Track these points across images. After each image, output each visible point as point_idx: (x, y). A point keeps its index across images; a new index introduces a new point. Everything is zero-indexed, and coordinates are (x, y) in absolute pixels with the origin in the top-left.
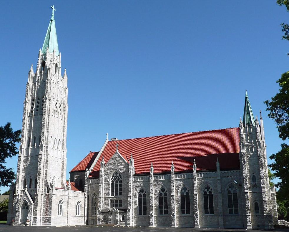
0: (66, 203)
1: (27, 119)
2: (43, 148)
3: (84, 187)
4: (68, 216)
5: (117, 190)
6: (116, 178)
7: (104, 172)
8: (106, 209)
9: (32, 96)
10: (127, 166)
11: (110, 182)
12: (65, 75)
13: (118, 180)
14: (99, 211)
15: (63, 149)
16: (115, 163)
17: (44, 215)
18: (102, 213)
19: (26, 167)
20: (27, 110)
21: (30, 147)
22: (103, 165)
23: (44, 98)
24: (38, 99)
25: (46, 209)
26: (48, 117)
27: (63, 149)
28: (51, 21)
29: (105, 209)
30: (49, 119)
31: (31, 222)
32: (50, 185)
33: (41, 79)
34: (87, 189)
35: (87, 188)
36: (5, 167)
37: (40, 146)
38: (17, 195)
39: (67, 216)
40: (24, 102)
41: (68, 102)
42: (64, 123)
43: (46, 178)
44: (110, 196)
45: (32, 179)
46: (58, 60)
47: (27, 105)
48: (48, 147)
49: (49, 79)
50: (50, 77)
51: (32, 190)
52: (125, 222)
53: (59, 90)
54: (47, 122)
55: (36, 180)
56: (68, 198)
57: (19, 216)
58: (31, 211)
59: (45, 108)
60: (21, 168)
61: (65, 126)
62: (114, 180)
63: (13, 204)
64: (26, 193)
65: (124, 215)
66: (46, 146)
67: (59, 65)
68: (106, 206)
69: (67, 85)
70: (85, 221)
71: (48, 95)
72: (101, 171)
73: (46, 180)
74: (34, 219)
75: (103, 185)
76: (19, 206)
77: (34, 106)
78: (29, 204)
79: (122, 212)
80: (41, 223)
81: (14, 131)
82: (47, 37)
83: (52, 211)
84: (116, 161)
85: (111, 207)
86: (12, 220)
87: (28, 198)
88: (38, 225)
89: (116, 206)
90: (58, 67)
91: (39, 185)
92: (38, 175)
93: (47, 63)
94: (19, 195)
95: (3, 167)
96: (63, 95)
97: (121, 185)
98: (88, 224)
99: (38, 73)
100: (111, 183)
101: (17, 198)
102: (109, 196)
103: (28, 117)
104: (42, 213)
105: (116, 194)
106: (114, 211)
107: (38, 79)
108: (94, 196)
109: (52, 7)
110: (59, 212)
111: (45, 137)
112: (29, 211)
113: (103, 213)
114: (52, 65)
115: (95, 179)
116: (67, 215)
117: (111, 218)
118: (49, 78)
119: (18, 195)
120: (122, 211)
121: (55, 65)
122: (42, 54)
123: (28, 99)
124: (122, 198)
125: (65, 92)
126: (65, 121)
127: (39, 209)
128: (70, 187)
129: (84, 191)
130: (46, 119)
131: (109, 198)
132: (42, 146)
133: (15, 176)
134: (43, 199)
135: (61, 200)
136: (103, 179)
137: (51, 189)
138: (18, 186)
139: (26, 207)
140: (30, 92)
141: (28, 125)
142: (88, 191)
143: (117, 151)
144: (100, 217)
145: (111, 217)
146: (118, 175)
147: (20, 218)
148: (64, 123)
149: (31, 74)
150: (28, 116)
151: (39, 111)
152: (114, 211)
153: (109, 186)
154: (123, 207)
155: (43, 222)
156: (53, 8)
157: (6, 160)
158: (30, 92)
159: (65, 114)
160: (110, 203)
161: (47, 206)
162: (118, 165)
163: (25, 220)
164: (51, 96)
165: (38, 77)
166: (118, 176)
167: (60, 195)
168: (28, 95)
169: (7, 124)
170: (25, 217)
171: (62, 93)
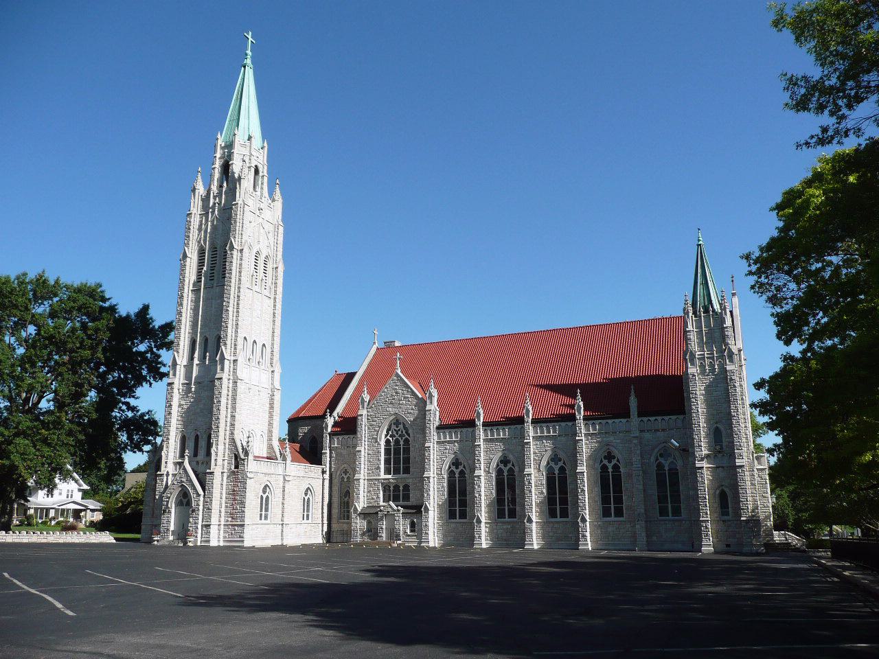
0: (278, 492)
1: (188, 297)
2: (226, 362)
5: (397, 462)
6: (395, 433)
7: (368, 419)
9: (199, 242)
10: (422, 405)
11: (383, 443)
13: (400, 438)
14: (356, 509)
16: (394, 399)
17: (227, 521)
18: (363, 516)
19: (185, 407)
20: (187, 275)
21: (196, 361)
22: (366, 404)
23: (227, 248)
24: (214, 249)
28: (245, 67)
29: (371, 505)
30: (238, 297)
31: (197, 537)
32: (241, 451)
33: (221, 202)
34: (328, 459)
35: (328, 456)
36: (136, 408)
37: (217, 359)
39: (281, 523)
41: (283, 256)
42: (275, 306)
44: (383, 476)
46: (261, 157)
47: (188, 264)
49: (239, 202)
50: (241, 199)
54: (236, 303)
55: (209, 437)
56: (285, 480)
57: (169, 522)
58: (199, 510)
59: (231, 270)
61: (276, 311)
63: (155, 495)
64: (185, 469)
65: (415, 520)
66: (233, 358)
67: (263, 171)
68: (373, 499)
69: (280, 218)
70: (324, 533)
71: (237, 239)
72: (359, 418)
73: (233, 439)
74: (204, 529)
77: (204, 265)
78: (193, 495)
80: (222, 539)
82: (235, 105)
83: (246, 510)
84: (397, 393)
85: (383, 502)
87: (191, 481)
88: (214, 543)
89: (396, 499)
90: (261, 174)
91: (215, 449)
92: (213, 427)
93: (234, 166)
94: (170, 473)
95: (133, 409)
96: (272, 240)
97: (407, 451)
99: (214, 188)
101: (165, 480)
103: (190, 291)
104: (223, 514)
105: (397, 471)
106: (390, 510)
107: (214, 204)
108: (343, 475)
109: (245, 34)
110: (263, 513)
111: (229, 338)
112: (193, 511)
113: (364, 515)
114: (246, 170)
115: (346, 437)
116: (282, 521)
117: (384, 527)
118: (239, 200)
119: (168, 472)
120: (410, 511)
121: (253, 170)
124: (409, 479)
125: (276, 234)
127: (215, 505)
128: (289, 455)
129: (321, 465)
130: (232, 296)
132: (223, 358)
133: (159, 430)
134: (225, 483)
135: (267, 486)
136: (365, 437)
137: (243, 460)
138: (168, 452)
139: (185, 500)
140: (194, 234)
141: (191, 309)
142: (330, 464)
143: (399, 371)
144: (359, 524)
145: (384, 525)
146: (401, 426)
147: (172, 528)
148: (275, 306)
149: (197, 191)
150: (191, 288)
151: (215, 278)
152: (390, 510)
153: (379, 452)
155: (225, 537)
156: (250, 37)
157: (139, 391)
158: (194, 234)
159: (276, 283)
160: (381, 492)
161: (235, 500)
162: (401, 402)
163: (183, 533)
164: (245, 243)
165: (215, 197)
168: (191, 239)
171: (271, 236)
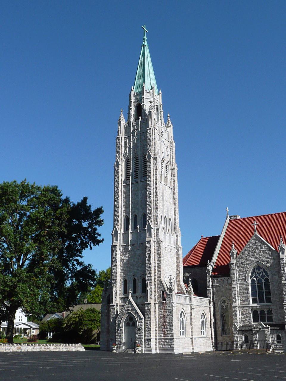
0: (188, 316)
1: (121, 190)
2: (152, 230)
3: (207, 290)
4: (194, 337)
5: (261, 294)
6: (257, 275)
7: (237, 266)
8: (246, 326)
9: (126, 155)
10: (276, 255)
11: (249, 282)
12: (170, 124)
13: (261, 278)
14: (236, 328)
15: (176, 233)
16: (255, 252)
17: (161, 336)
18: (241, 332)
19: (125, 261)
20: (120, 176)
21: (130, 231)
22: (235, 256)
23: (146, 157)
24: (136, 159)
25: (164, 325)
26: (155, 185)
27: (176, 233)
28: (144, 46)
29: (245, 324)
30: (156, 188)
31: (142, 347)
32: (166, 289)
33: (138, 129)
34: (212, 294)
35: (211, 292)
36: (82, 263)
37: (146, 228)
38: (116, 304)
39: (191, 337)
40: (115, 165)
41: (176, 161)
42: (174, 194)
43: (159, 277)
44: (252, 304)
45: (128, 281)
46: (159, 100)
47: (120, 169)
48: (159, 229)
49: (152, 128)
50: (152, 126)
51: (139, 298)
52: (282, 345)
53: (163, 144)
54: (155, 192)
55: (144, 280)
56: (191, 308)
57: (121, 337)
58: (142, 329)
59: (150, 171)
60: (119, 262)
61: (175, 197)
62: (255, 279)
63: (110, 319)
64: (130, 302)
65: (280, 335)
66: (156, 228)
67: (161, 109)
68: (246, 320)
69: (173, 137)
70: (213, 344)
71: (152, 151)
72: (232, 265)
73: (161, 281)
74: (147, 342)
75: (237, 286)
76: (120, 321)
77: (130, 169)
78: (137, 319)
79: (276, 330)
80: (158, 349)
81: (93, 209)
82: (140, 69)
83: (174, 329)
84: (257, 248)
85: (254, 322)
86: (111, 343)
87: (135, 309)
88: (154, 352)
89: (263, 320)
90: (159, 111)
91: (115, 290)
92: (147, 273)
93: (145, 106)
94: (119, 304)
95: (80, 264)
96: (169, 152)
97: (268, 286)
98: (218, 348)
99: (132, 120)
100: (251, 284)
101: (116, 309)
102: (249, 304)
103: (122, 186)
104: (157, 332)
105: (261, 301)
106: (261, 327)
107: (134, 130)
108: (223, 304)
109: (143, 27)
110: (181, 330)
111: (153, 214)
112: (139, 330)
113: (242, 331)
114: (153, 107)
115: (223, 278)
116: (192, 336)
117: (258, 339)
118: (151, 126)
119: (117, 304)
120: (276, 328)
121: (156, 107)
122: (135, 94)
123: (120, 160)
124: (272, 306)
125: (171, 148)
126: (176, 190)
127: (153, 324)
128: (193, 291)
129: (207, 297)
130: (152, 188)
131: (249, 307)
132: (150, 228)
133: (96, 277)
134: (157, 311)
135: (182, 312)
136: (237, 278)
137: (169, 295)
138: (116, 291)
139: (131, 322)
140: (122, 150)
141: (124, 197)
142: (213, 297)
143: (257, 234)
144: (239, 338)
145: (257, 338)
146: (262, 270)
147: (123, 341)
148: (174, 194)
149: (122, 124)
150: (123, 184)
151: (139, 177)
152: (261, 327)
153: (248, 288)
154: (276, 321)
155: (160, 347)
156: (145, 28)
157: (84, 252)
158: (122, 150)
159: (174, 179)
160: (252, 315)
161: (165, 322)
162: (260, 254)
163: (132, 344)
164: (157, 153)
165: (134, 126)
166: (260, 273)
167: (181, 304)
168: (120, 153)
169: (82, 199)
170: (131, 339)
171: (168, 148)
